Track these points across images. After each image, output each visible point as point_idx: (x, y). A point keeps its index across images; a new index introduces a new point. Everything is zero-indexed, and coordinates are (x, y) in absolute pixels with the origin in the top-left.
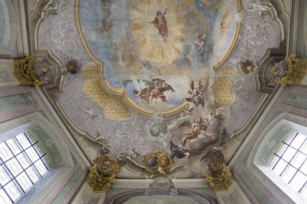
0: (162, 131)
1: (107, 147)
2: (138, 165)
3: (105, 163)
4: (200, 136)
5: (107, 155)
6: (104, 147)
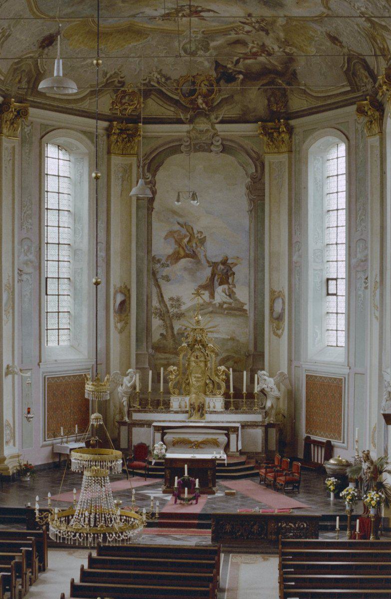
0: (201, 48)
1: (120, 80)
2: (169, 94)
3: (124, 101)
5: (123, 89)
6: (116, 82)
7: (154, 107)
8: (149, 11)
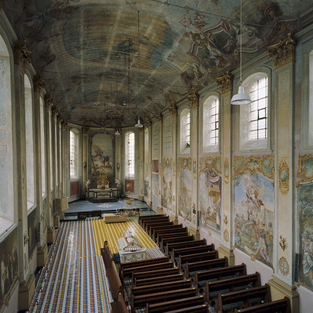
4: (116, 115)
7: (92, 124)
8: (95, 103)
